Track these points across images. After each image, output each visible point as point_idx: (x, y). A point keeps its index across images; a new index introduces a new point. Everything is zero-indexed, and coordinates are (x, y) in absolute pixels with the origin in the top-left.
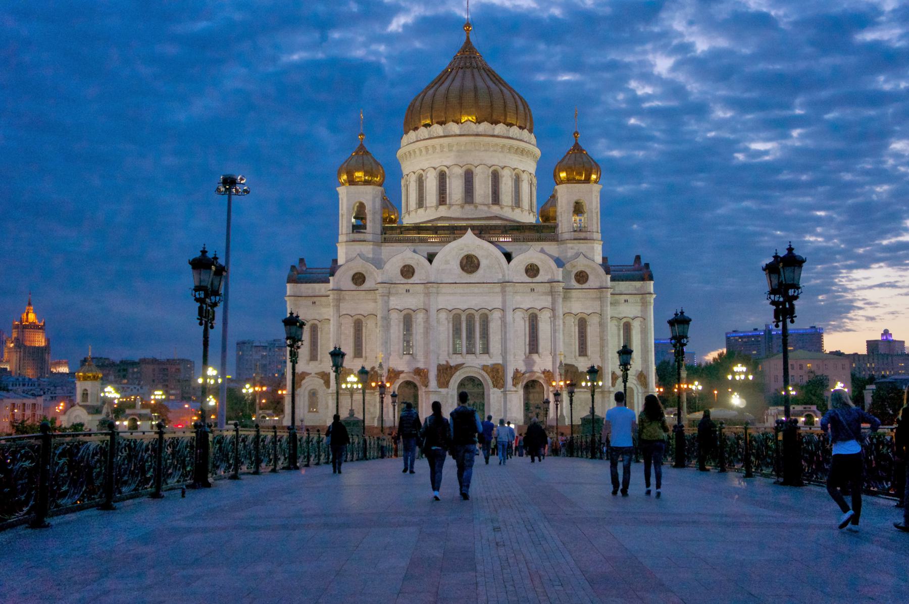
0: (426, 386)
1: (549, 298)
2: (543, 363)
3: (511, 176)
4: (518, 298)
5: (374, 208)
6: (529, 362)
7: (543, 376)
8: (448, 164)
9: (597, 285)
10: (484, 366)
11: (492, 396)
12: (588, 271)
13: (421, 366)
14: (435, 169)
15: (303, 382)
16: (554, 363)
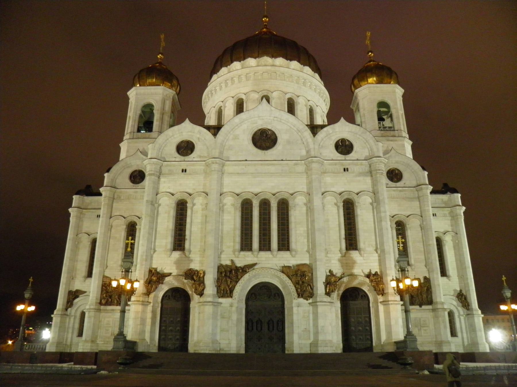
0: (201, 294)
1: (368, 180)
2: (365, 262)
3: (306, 105)
4: (328, 179)
5: (163, 108)
6: (347, 264)
7: (367, 280)
8: (245, 91)
9: (414, 183)
10: (284, 267)
11: (295, 309)
12: (401, 168)
13: (195, 266)
14: (233, 97)
15: (76, 300)
16: (382, 261)
